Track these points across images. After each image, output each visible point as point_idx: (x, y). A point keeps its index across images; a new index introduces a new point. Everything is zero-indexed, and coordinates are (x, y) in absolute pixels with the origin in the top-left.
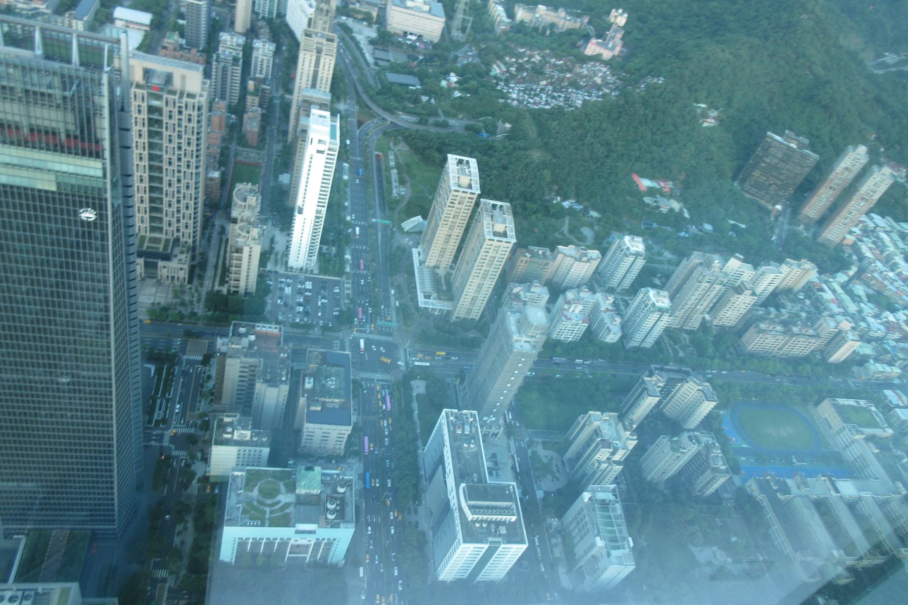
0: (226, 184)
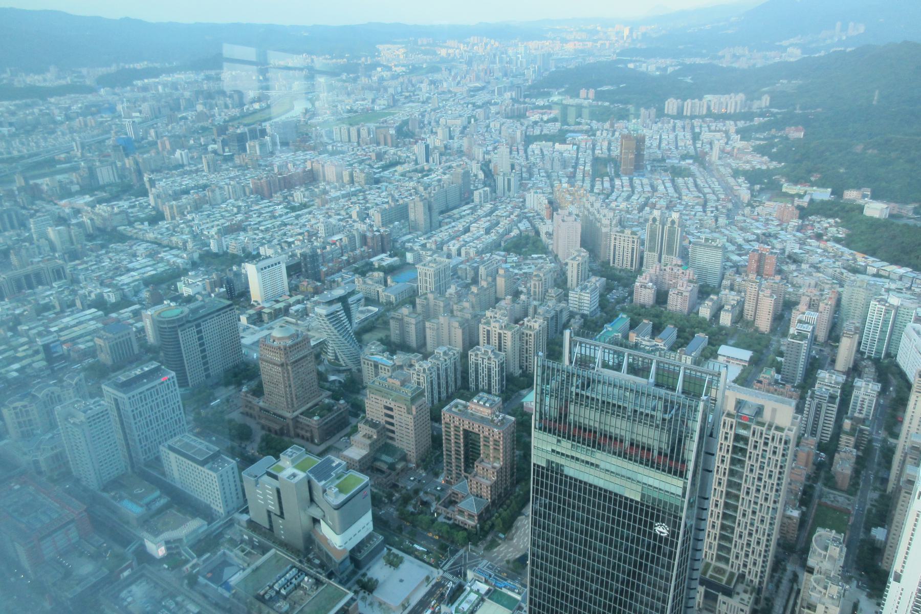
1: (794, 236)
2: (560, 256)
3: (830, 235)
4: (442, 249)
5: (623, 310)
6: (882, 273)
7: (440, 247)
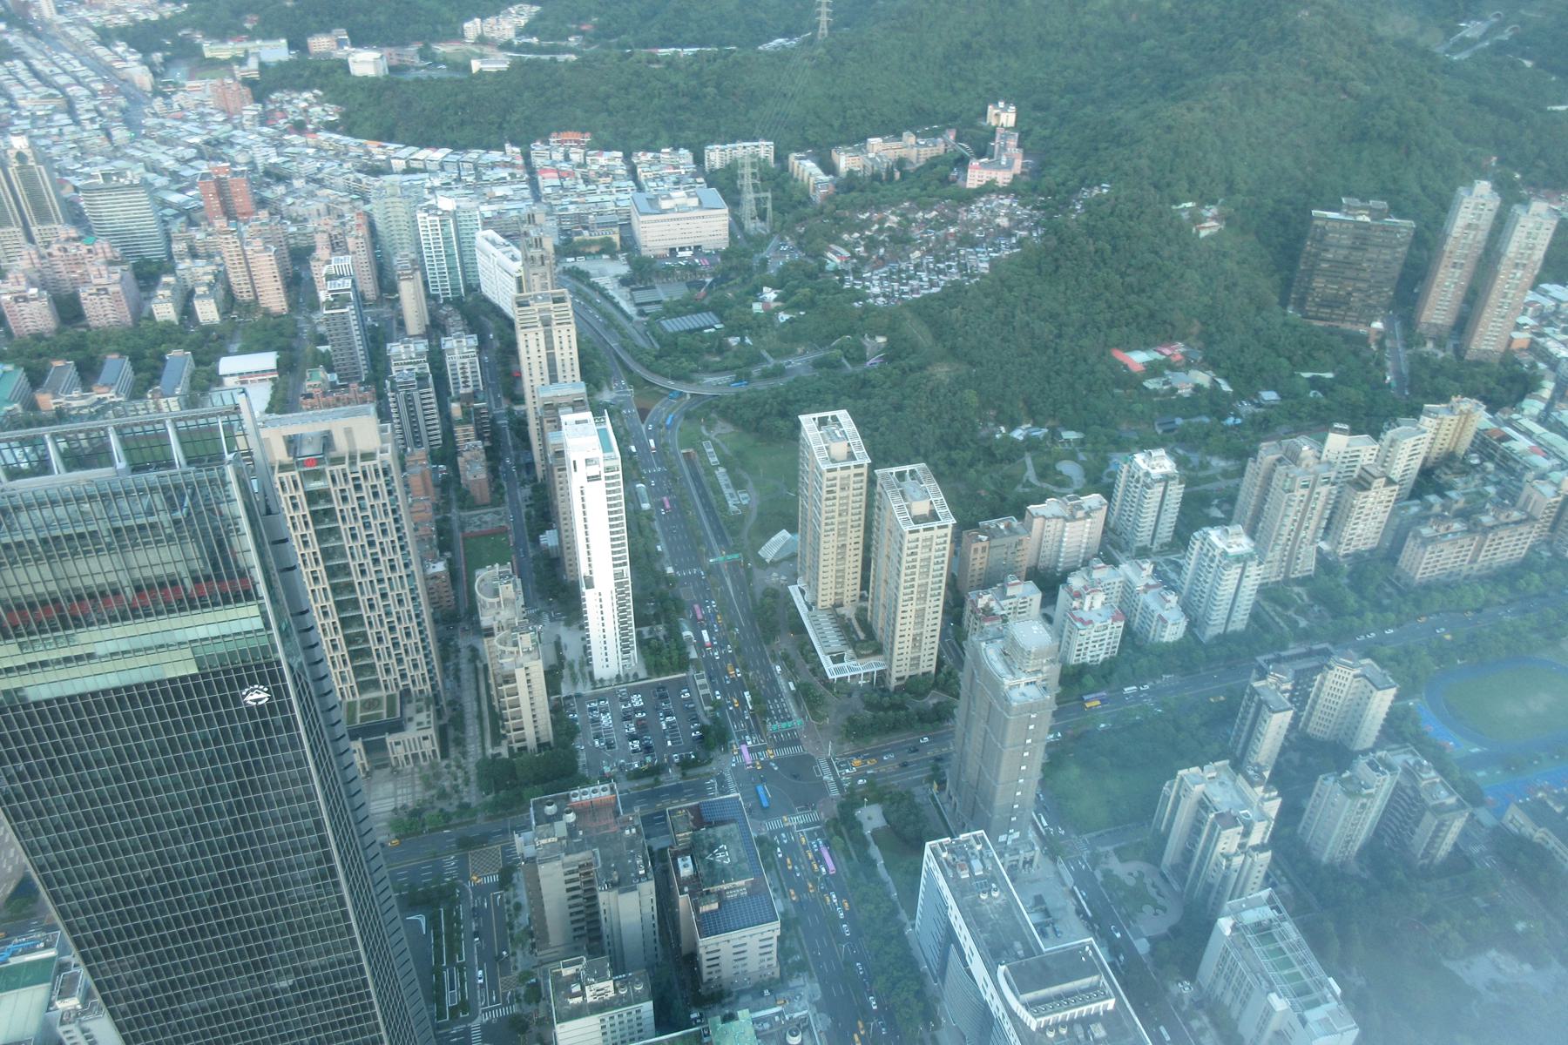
0: (459, 578)
1: (260, 134)
3: (316, 121)
6: (415, 165)
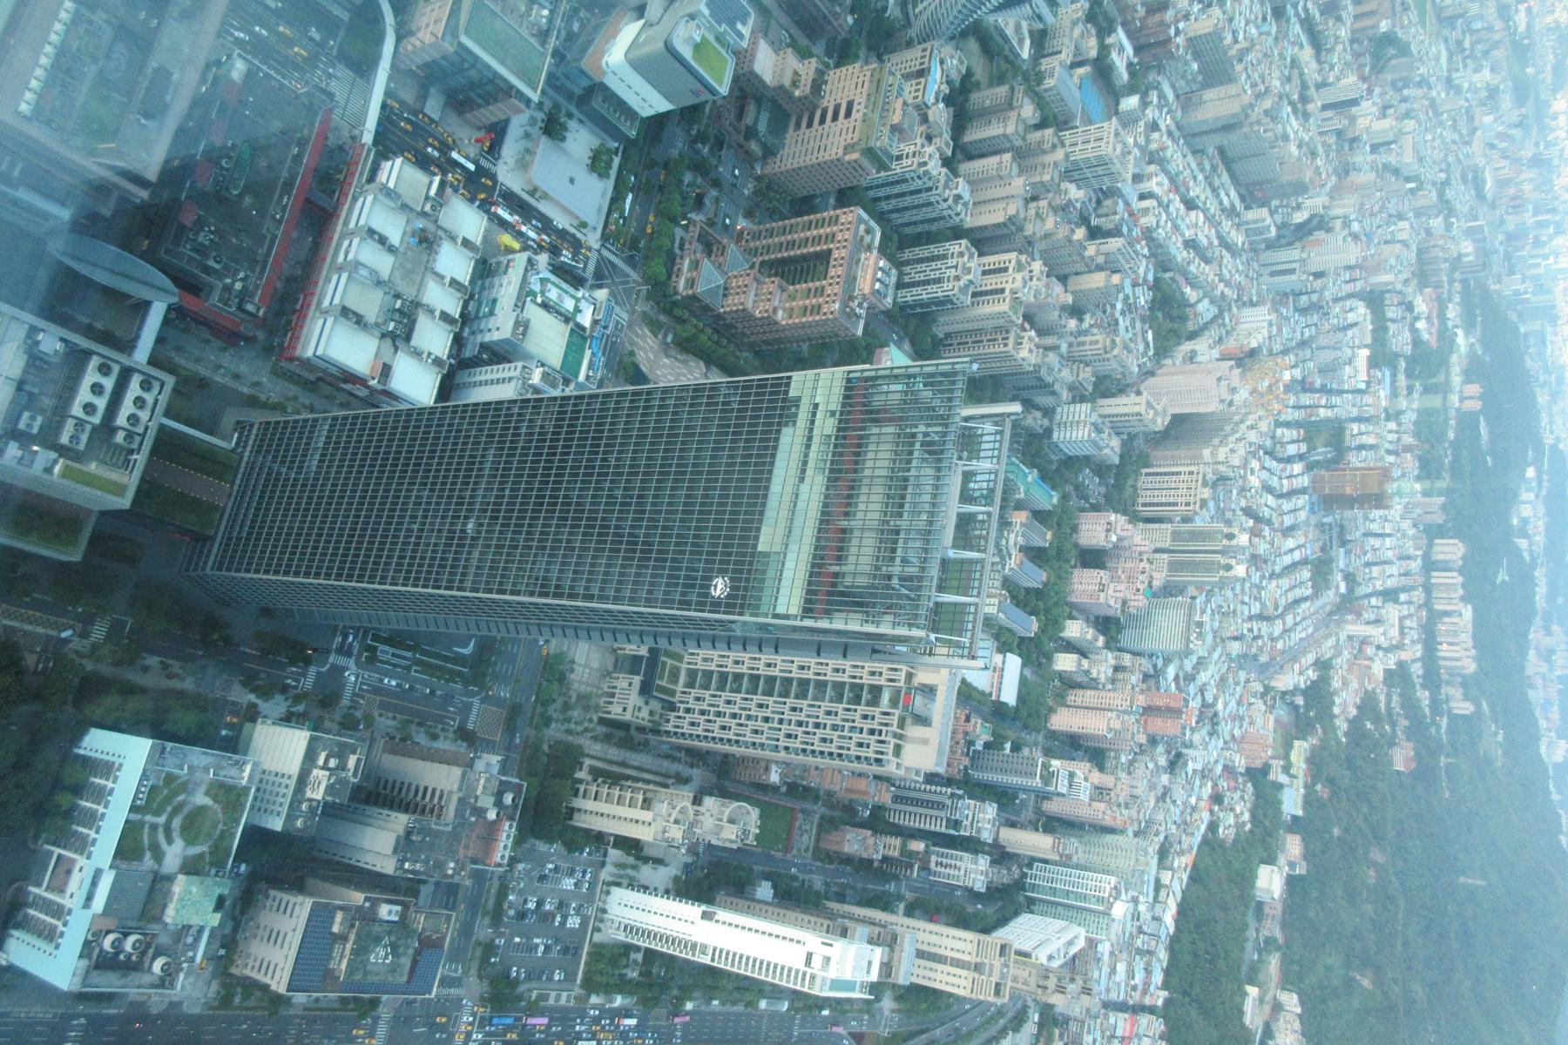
0: (757, 792)
1: (1216, 762)
2: (1152, 381)
3: (1221, 815)
4: (1150, 162)
5: (1065, 498)
6: (1163, 893)
7: (1154, 158)
